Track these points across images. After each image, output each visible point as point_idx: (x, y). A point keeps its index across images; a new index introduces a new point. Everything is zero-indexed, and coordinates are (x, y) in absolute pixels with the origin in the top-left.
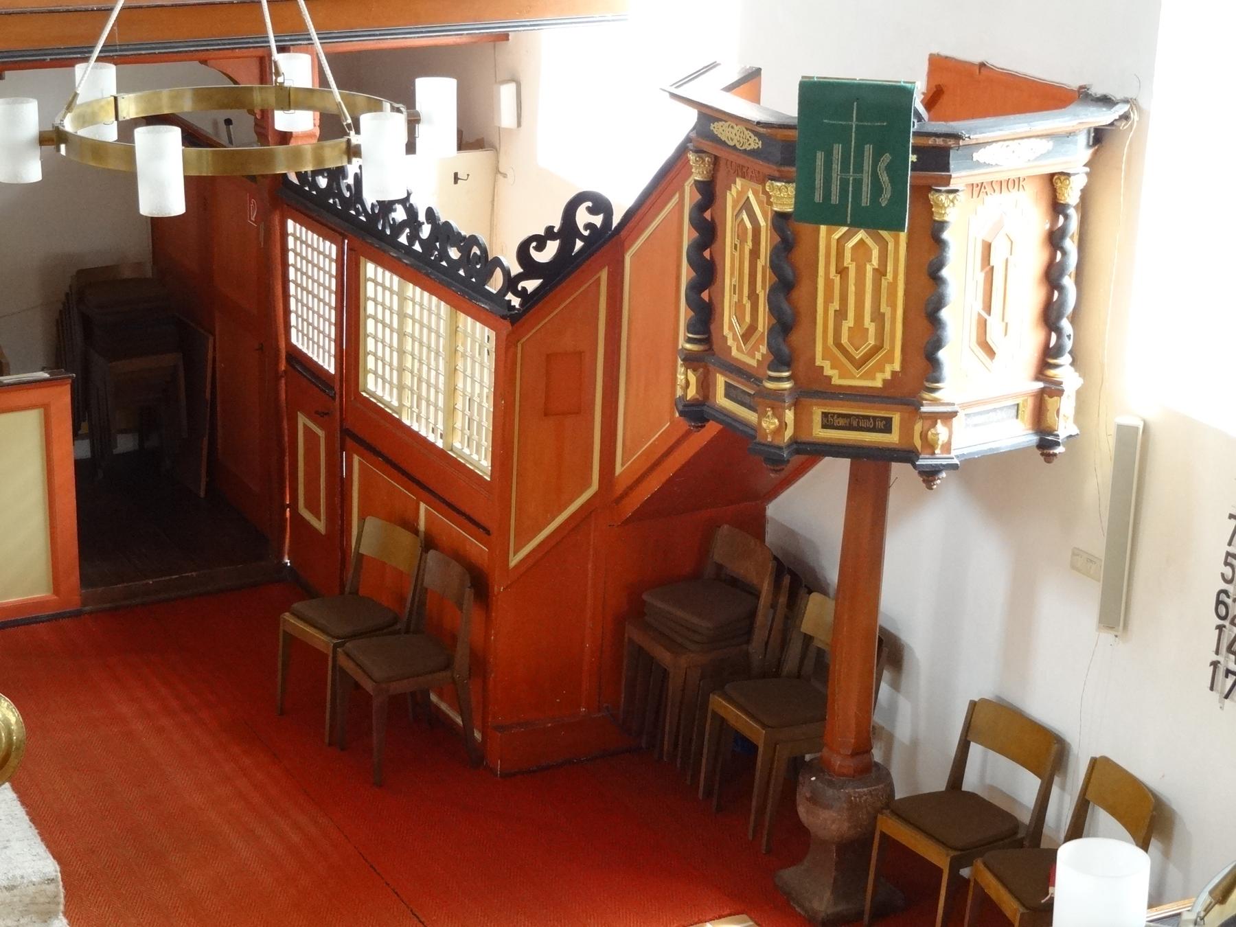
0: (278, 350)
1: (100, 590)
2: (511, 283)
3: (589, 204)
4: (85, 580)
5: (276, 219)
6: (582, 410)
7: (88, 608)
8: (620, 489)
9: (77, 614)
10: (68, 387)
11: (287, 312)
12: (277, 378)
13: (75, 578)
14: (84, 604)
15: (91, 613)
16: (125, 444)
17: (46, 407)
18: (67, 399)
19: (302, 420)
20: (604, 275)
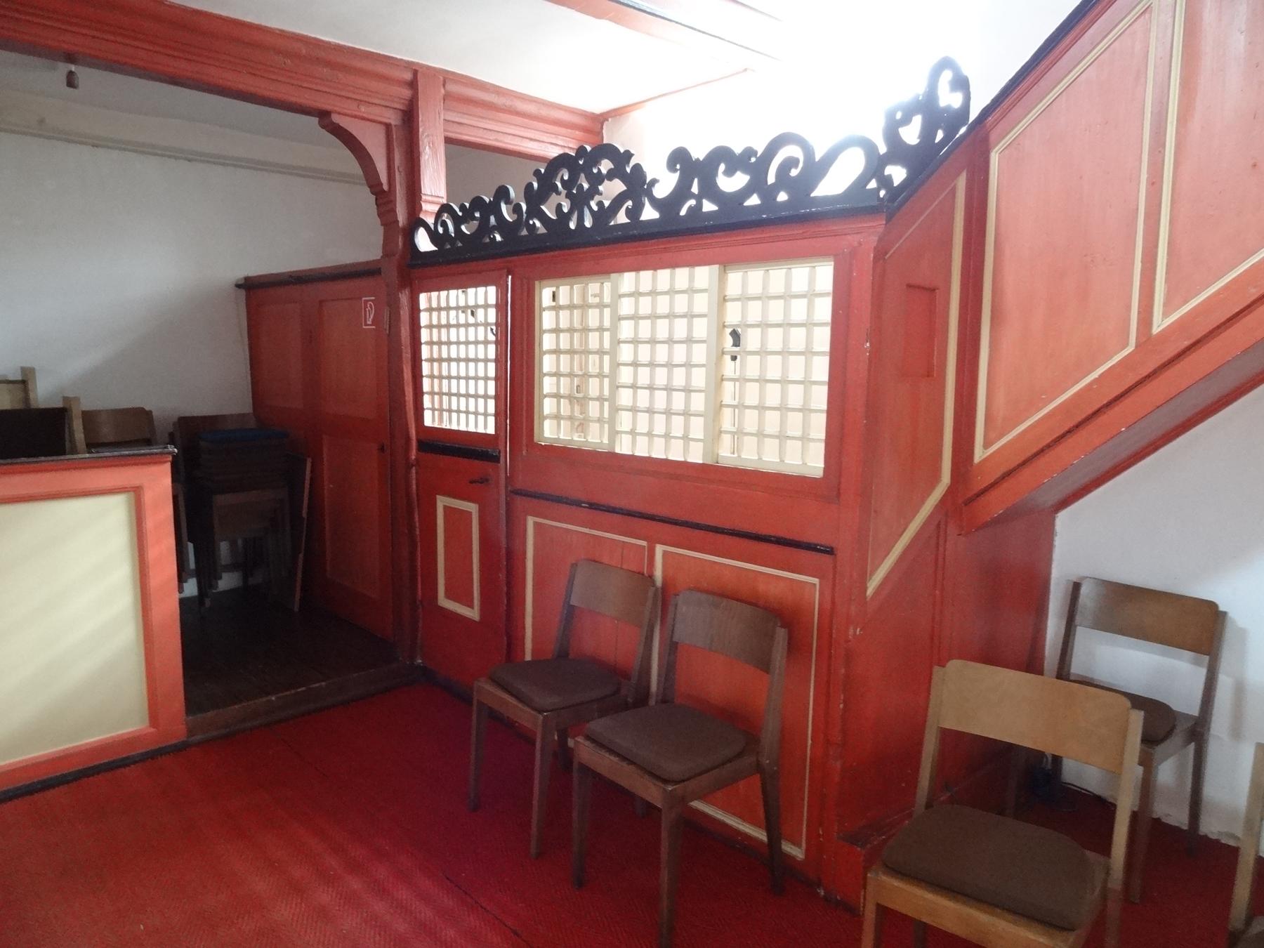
0: (408, 439)
1: (210, 714)
2: (876, 167)
3: (947, 76)
4: (192, 705)
5: (404, 298)
6: (933, 373)
7: (199, 737)
8: (981, 482)
9: (178, 749)
10: (167, 467)
11: (418, 393)
12: (409, 466)
13: (178, 701)
14: (191, 732)
15: (199, 744)
16: (227, 582)
17: (137, 493)
18: (167, 481)
19: (442, 502)
20: (961, 183)
